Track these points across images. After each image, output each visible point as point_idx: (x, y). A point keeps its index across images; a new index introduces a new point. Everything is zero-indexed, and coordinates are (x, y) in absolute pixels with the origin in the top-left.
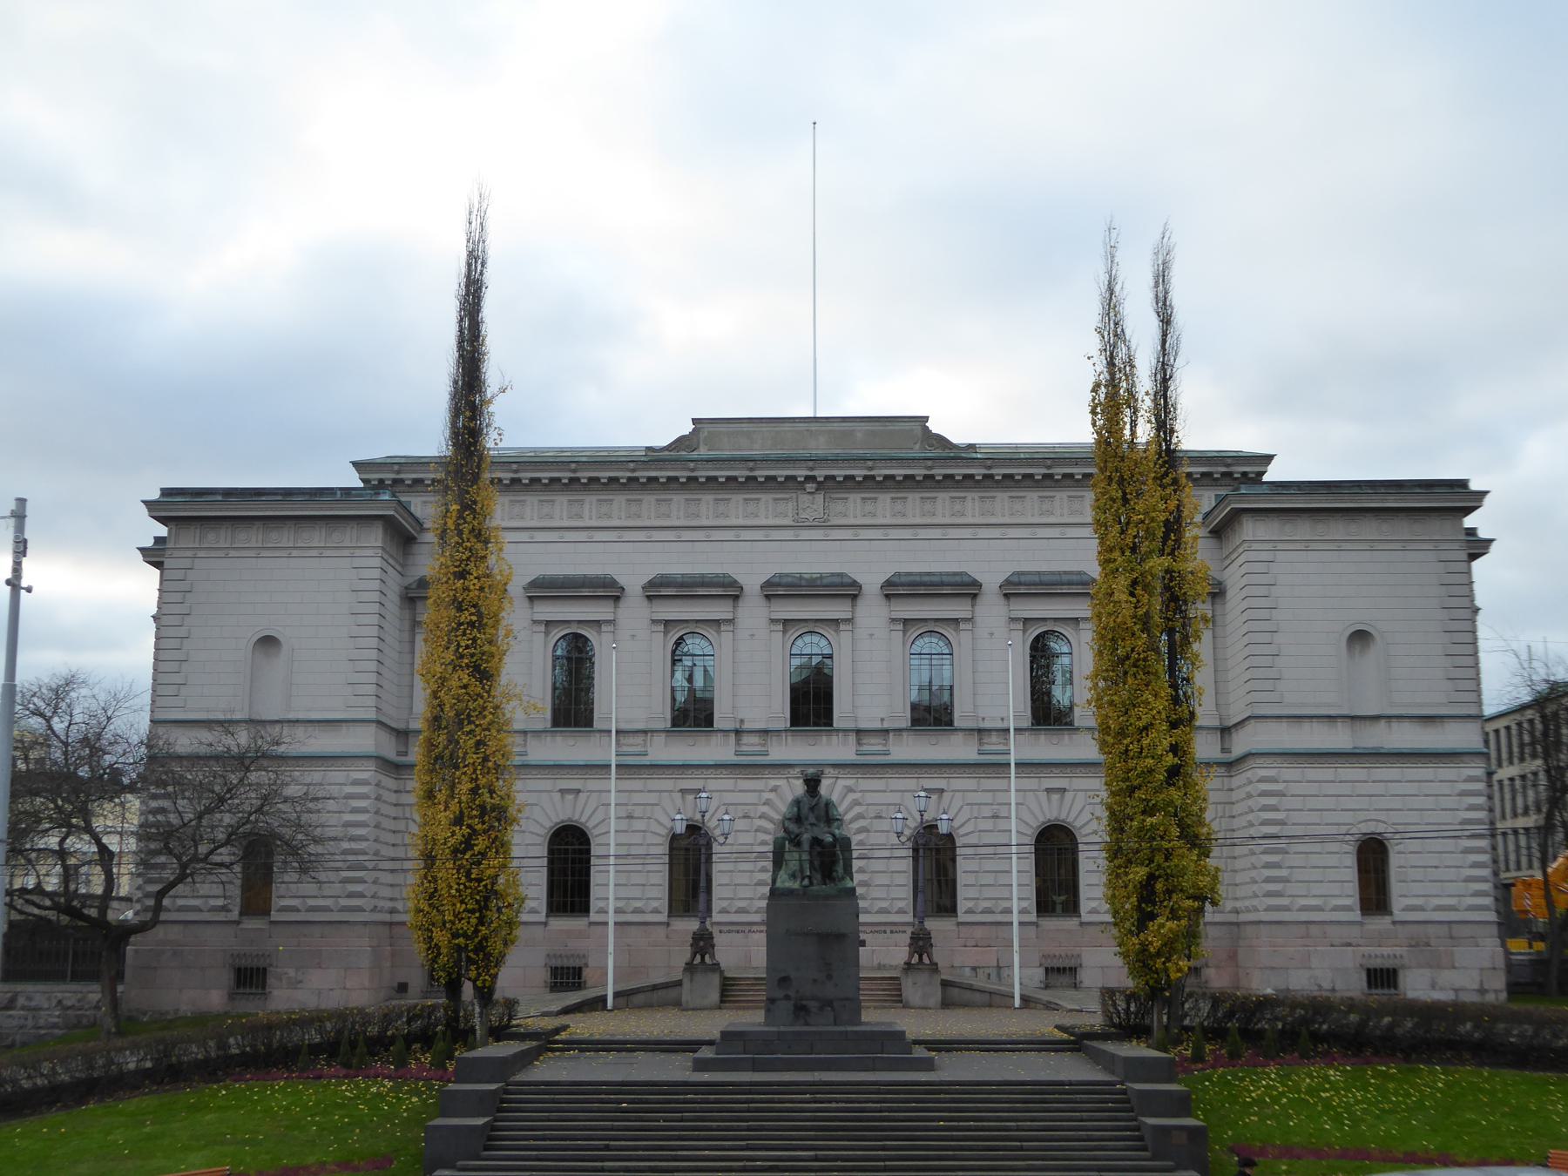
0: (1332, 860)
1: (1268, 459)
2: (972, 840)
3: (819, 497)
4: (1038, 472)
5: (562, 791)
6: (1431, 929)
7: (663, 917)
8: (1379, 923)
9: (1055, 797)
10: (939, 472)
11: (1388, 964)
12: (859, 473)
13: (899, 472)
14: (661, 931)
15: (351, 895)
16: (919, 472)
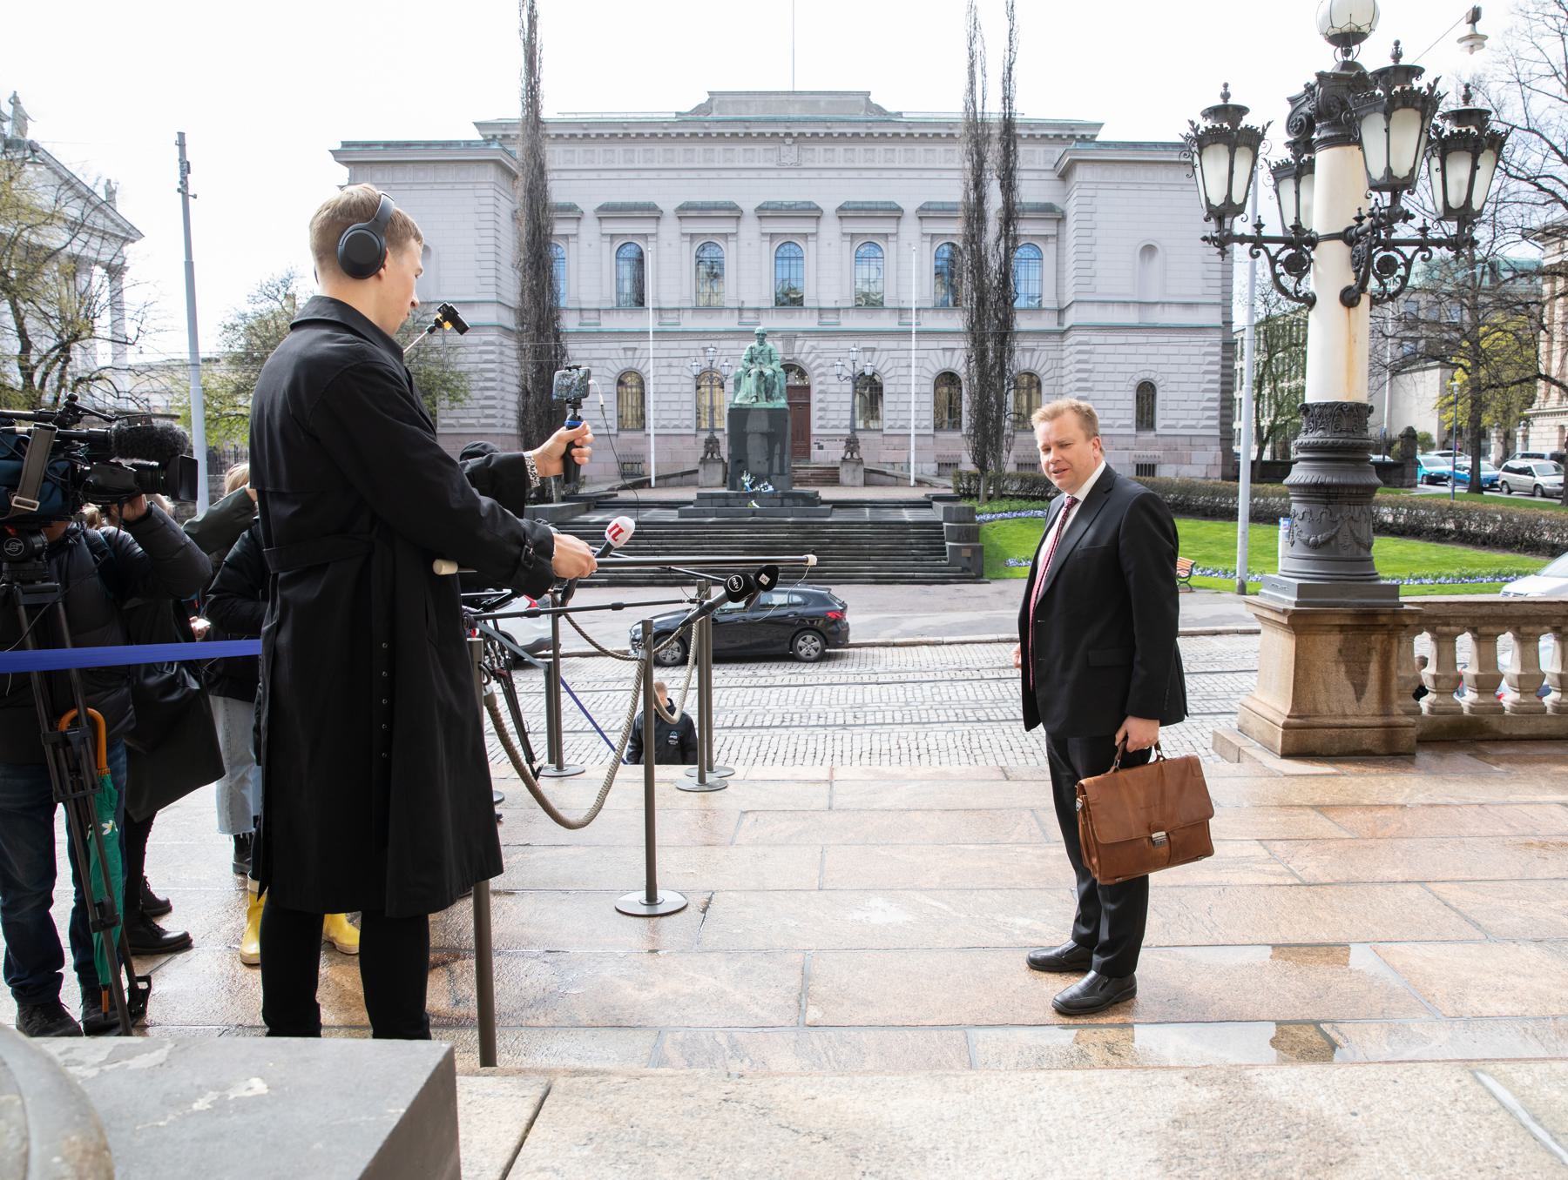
0: (1120, 396)
2: (894, 381)
3: (795, 148)
4: (944, 131)
5: (625, 349)
6: (1179, 440)
7: (693, 431)
8: (1148, 436)
9: (948, 354)
10: (876, 131)
11: (1150, 462)
12: (822, 131)
13: (849, 130)
14: (692, 439)
16: (862, 130)
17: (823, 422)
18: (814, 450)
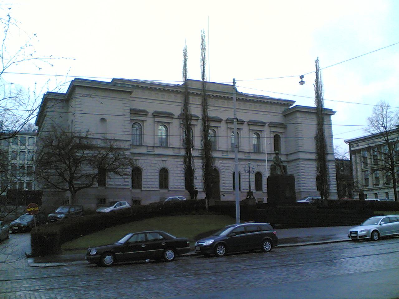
0: (312, 180)
1: (295, 101)
3: (214, 100)
12: (222, 95)
15: (126, 182)
17: (224, 187)
18: (222, 196)
